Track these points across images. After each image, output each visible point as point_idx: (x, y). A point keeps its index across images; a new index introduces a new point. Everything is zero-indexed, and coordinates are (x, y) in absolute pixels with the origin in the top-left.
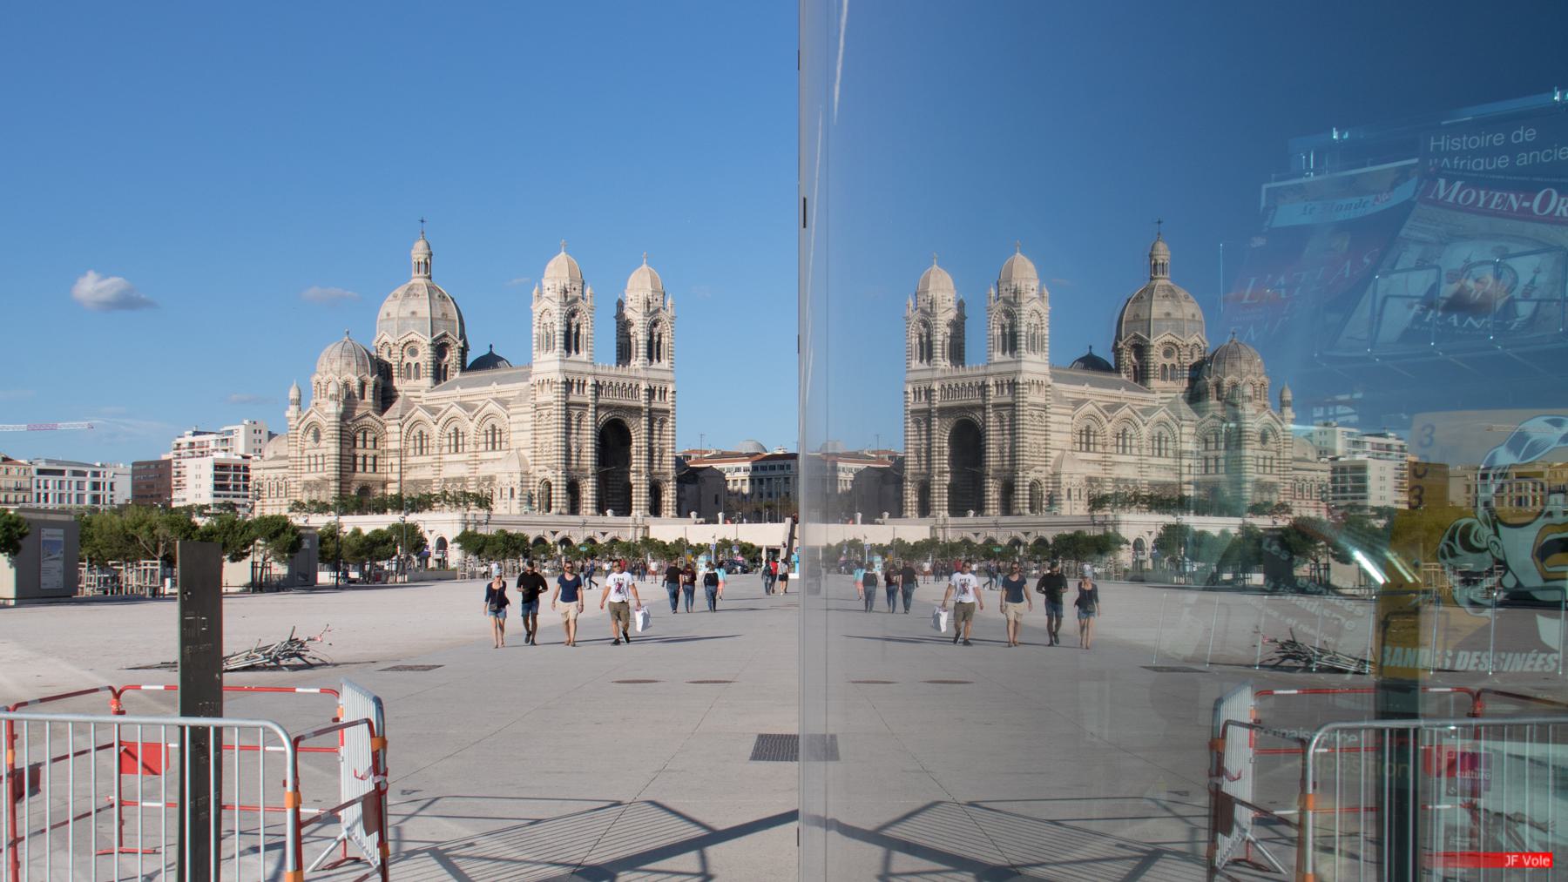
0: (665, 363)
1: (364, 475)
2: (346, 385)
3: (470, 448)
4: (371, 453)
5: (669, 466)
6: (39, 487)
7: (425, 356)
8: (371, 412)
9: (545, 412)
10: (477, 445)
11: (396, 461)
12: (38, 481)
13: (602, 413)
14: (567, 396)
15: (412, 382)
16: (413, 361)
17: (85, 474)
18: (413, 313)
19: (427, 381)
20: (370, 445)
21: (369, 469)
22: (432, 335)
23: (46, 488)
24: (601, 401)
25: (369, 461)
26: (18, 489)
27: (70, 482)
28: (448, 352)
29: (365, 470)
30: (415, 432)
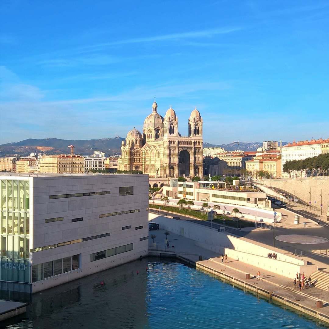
0: (200, 135)
1: (137, 163)
2: (132, 141)
3: (155, 157)
4: (139, 158)
5: (201, 162)
6: (86, 163)
7: (153, 133)
8: (138, 147)
9: (165, 149)
10: (156, 156)
11: (143, 159)
12: (86, 162)
13: (180, 149)
14: (170, 145)
15: (150, 139)
16: (151, 134)
17: (97, 160)
18: (151, 122)
19: (153, 139)
20: (138, 155)
21: (138, 161)
22: (155, 127)
23: (88, 163)
24: (180, 146)
25: (138, 160)
26: (81, 164)
27: (93, 162)
28: (160, 131)
29: (137, 162)
30: (147, 153)
